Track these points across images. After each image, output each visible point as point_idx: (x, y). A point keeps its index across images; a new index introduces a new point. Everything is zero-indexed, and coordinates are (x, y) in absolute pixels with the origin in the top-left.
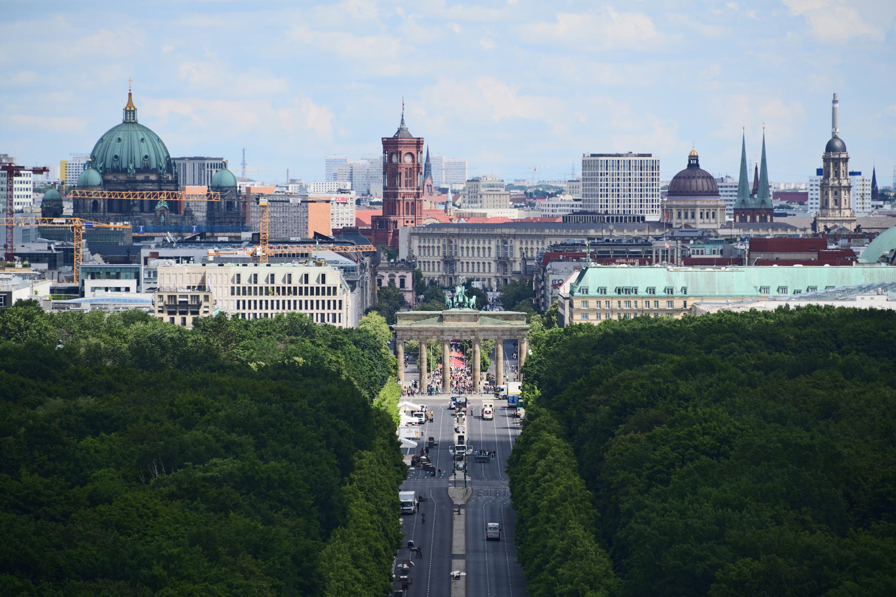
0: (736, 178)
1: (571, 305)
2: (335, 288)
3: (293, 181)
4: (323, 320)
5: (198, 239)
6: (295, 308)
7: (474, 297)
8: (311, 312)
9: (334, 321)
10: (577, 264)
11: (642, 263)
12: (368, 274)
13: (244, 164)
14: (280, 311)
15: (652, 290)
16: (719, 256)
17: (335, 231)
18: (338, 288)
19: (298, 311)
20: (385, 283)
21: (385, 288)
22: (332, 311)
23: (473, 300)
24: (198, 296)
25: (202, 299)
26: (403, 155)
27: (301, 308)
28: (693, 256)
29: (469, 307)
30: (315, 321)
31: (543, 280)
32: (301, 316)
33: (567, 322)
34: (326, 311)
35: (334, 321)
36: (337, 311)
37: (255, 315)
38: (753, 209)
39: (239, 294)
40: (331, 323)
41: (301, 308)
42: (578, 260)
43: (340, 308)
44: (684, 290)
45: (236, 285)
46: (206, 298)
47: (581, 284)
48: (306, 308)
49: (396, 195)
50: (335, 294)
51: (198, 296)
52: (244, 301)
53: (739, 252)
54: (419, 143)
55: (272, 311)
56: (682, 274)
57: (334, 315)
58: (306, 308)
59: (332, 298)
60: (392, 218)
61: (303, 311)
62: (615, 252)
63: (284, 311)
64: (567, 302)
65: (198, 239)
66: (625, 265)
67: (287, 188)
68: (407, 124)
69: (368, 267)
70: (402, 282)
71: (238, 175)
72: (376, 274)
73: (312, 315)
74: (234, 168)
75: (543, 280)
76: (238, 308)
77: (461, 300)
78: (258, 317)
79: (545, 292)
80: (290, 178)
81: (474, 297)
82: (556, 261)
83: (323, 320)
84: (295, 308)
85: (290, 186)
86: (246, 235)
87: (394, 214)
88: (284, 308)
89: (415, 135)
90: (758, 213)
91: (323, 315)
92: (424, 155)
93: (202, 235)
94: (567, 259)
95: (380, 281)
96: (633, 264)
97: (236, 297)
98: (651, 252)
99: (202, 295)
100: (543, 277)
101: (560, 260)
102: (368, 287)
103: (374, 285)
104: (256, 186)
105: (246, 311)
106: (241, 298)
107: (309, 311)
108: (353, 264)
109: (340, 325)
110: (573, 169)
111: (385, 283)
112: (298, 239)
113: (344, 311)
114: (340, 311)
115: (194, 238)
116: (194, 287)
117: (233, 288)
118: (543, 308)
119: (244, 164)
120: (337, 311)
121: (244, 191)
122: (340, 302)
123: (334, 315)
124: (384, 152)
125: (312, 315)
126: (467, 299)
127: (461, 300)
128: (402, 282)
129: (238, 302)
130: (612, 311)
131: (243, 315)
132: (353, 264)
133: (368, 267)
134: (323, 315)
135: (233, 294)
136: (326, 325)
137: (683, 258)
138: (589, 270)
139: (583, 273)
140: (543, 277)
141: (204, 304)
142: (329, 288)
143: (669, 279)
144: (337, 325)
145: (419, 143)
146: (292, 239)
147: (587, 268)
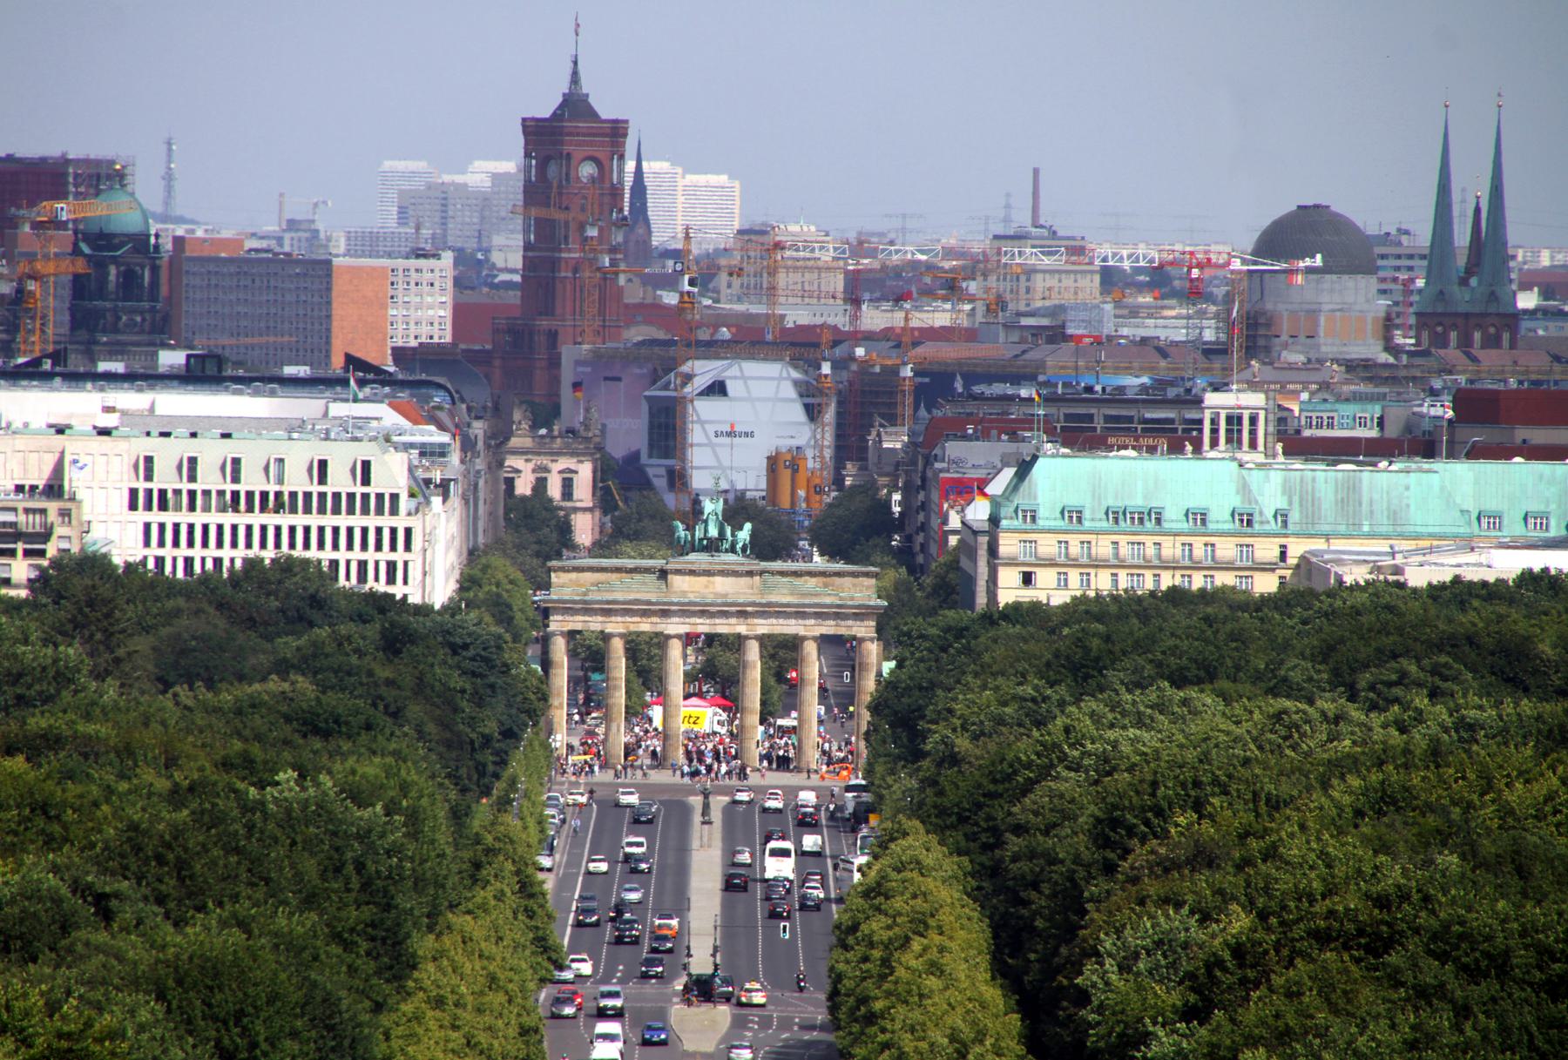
0: (1423, 236)
1: (993, 551)
2: (395, 497)
3: (292, 225)
4: (362, 578)
5: (47, 365)
6: (292, 546)
7: (748, 526)
8: (334, 555)
9: (391, 580)
10: (1011, 447)
11: (1176, 449)
12: (480, 464)
13: (169, 177)
14: (255, 551)
15: (1199, 517)
16: (1374, 433)
17: (400, 354)
18: (404, 497)
19: (299, 552)
20: (523, 487)
21: (524, 498)
22: (385, 555)
23: (744, 534)
24: (43, 511)
25: (52, 516)
26: (573, 162)
27: (307, 546)
28: (1307, 433)
29: (733, 550)
30: (342, 581)
31: (923, 487)
32: (307, 562)
33: (981, 600)
34: (370, 556)
35: (391, 580)
36: (399, 556)
37: (189, 562)
38: (1467, 315)
39: (148, 507)
40: (381, 587)
41: (307, 546)
42: (1014, 437)
43: (408, 547)
44: (1282, 516)
45: (142, 485)
46: (65, 514)
47: (1020, 499)
48: (321, 546)
49: (554, 264)
50: (394, 511)
51: (43, 511)
52: (162, 527)
53: (1426, 425)
54: (617, 131)
55: (234, 553)
56: (1276, 477)
57: (392, 566)
58: (321, 546)
59: (386, 522)
60: (544, 323)
61: (313, 553)
62: (1108, 419)
63: (264, 554)
64: (983, 540)
65: (47, 365)
66: (1131, 453)
67: (280, 240)
68: (586, 87)
69: (480, 444)
70: (567, 486)
71: (153, 203)
72: (501, 464)
73: (334, 564)
74: (146, 189)
75: (923, 487)
76: (147, 544)
77: (713, 532)
78: (197, 568)
79: (928, 518)
80: (287, 215)
81: (748, 526)
82: (956, 438)
83: (362, 578)
84: (292, 546)
85: (287, 236)
86: (171, 359)
87: (549, 311)
88: (263, 545)
89: (606, 111)
90: (1479, 326)
91: (362, 565)
92: (630, 166)
93: (58, 357)
94: (983, 435)
95: (510, 483)
96: (1152, 450)
97: (141, 516)
98: (1200, 422)
99: (53, 507)
100: (924, 479)
101: (965, 437)
102: (481, 495)
103: (494, 491)
104: (200, 233)
105: (167, 552)
106: (155, 517)
107: (327, 554)
108: (444, 438)
109: (406, 590)
110: (1008, 206)
111: (523, 487)
112: (302, 371)
113: (414, 557)
114: (407, 556)
115: (36, 362)
116: (33, 488)
117: (133, 493)
118: (920, 559)
119: (169, 177)
120: (399, 556)
121: (167, 245)
122: (408, 531)
123: (392, 566)
124: (527, 155)
125: (334, 564)
126: (728, 530)
127: (713, 532)
128: (567, 486)
129: (147, 526)
130: (1099, 564)
131: (160, 561)
132: (444, 438)
133: (480, 444)
134: (362, 565)
135: (133, 506)
136: (372, 595)
137: (1281, 435)
138: (1041, 462)
139: (1024, 468)
140: (924, 479)
141: (59, 530)
142: (380, 497)
143: (1244, 489)
144: (398, 590)
145: (617, 131)
146: (289, 370)
147: (1035, 458)
